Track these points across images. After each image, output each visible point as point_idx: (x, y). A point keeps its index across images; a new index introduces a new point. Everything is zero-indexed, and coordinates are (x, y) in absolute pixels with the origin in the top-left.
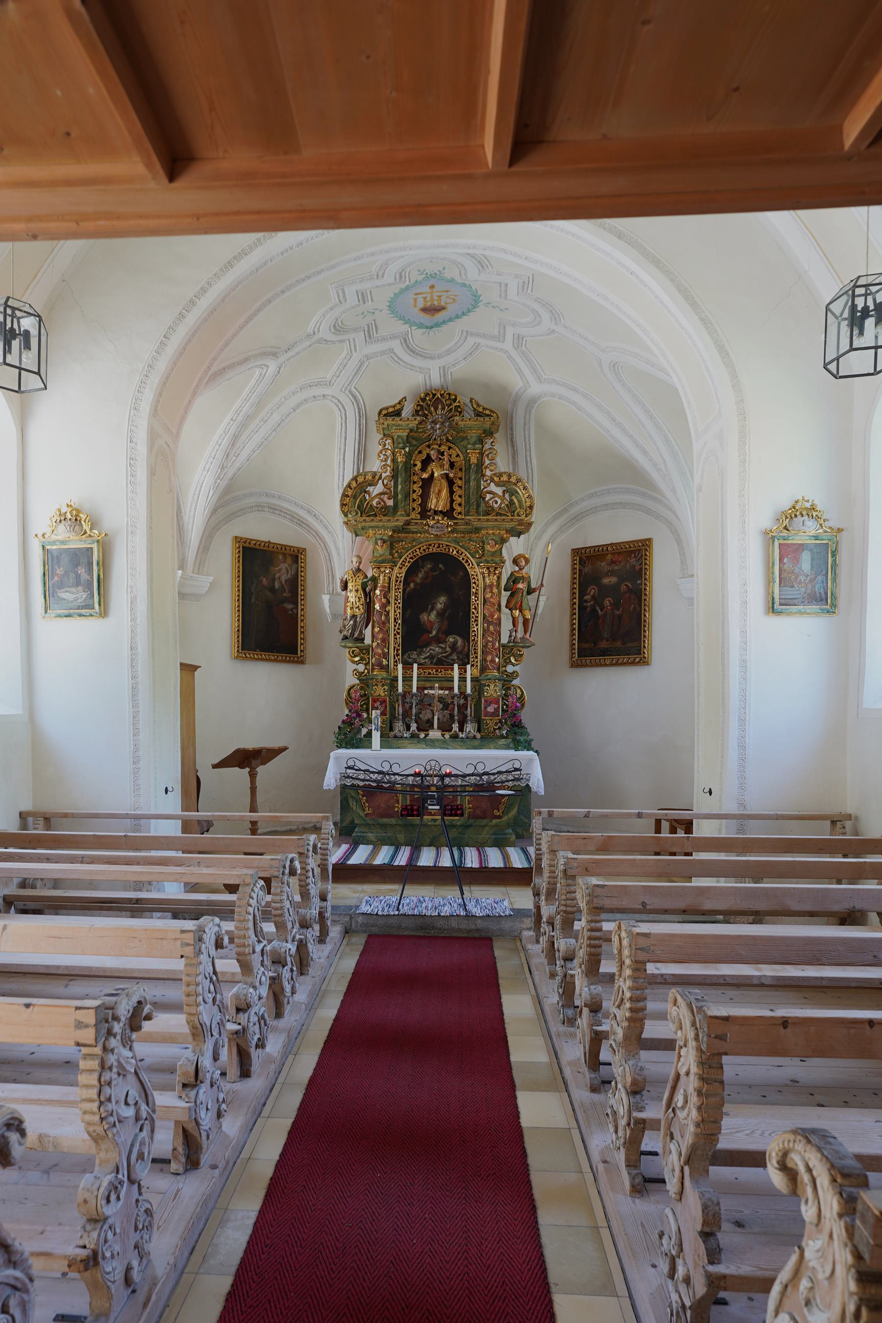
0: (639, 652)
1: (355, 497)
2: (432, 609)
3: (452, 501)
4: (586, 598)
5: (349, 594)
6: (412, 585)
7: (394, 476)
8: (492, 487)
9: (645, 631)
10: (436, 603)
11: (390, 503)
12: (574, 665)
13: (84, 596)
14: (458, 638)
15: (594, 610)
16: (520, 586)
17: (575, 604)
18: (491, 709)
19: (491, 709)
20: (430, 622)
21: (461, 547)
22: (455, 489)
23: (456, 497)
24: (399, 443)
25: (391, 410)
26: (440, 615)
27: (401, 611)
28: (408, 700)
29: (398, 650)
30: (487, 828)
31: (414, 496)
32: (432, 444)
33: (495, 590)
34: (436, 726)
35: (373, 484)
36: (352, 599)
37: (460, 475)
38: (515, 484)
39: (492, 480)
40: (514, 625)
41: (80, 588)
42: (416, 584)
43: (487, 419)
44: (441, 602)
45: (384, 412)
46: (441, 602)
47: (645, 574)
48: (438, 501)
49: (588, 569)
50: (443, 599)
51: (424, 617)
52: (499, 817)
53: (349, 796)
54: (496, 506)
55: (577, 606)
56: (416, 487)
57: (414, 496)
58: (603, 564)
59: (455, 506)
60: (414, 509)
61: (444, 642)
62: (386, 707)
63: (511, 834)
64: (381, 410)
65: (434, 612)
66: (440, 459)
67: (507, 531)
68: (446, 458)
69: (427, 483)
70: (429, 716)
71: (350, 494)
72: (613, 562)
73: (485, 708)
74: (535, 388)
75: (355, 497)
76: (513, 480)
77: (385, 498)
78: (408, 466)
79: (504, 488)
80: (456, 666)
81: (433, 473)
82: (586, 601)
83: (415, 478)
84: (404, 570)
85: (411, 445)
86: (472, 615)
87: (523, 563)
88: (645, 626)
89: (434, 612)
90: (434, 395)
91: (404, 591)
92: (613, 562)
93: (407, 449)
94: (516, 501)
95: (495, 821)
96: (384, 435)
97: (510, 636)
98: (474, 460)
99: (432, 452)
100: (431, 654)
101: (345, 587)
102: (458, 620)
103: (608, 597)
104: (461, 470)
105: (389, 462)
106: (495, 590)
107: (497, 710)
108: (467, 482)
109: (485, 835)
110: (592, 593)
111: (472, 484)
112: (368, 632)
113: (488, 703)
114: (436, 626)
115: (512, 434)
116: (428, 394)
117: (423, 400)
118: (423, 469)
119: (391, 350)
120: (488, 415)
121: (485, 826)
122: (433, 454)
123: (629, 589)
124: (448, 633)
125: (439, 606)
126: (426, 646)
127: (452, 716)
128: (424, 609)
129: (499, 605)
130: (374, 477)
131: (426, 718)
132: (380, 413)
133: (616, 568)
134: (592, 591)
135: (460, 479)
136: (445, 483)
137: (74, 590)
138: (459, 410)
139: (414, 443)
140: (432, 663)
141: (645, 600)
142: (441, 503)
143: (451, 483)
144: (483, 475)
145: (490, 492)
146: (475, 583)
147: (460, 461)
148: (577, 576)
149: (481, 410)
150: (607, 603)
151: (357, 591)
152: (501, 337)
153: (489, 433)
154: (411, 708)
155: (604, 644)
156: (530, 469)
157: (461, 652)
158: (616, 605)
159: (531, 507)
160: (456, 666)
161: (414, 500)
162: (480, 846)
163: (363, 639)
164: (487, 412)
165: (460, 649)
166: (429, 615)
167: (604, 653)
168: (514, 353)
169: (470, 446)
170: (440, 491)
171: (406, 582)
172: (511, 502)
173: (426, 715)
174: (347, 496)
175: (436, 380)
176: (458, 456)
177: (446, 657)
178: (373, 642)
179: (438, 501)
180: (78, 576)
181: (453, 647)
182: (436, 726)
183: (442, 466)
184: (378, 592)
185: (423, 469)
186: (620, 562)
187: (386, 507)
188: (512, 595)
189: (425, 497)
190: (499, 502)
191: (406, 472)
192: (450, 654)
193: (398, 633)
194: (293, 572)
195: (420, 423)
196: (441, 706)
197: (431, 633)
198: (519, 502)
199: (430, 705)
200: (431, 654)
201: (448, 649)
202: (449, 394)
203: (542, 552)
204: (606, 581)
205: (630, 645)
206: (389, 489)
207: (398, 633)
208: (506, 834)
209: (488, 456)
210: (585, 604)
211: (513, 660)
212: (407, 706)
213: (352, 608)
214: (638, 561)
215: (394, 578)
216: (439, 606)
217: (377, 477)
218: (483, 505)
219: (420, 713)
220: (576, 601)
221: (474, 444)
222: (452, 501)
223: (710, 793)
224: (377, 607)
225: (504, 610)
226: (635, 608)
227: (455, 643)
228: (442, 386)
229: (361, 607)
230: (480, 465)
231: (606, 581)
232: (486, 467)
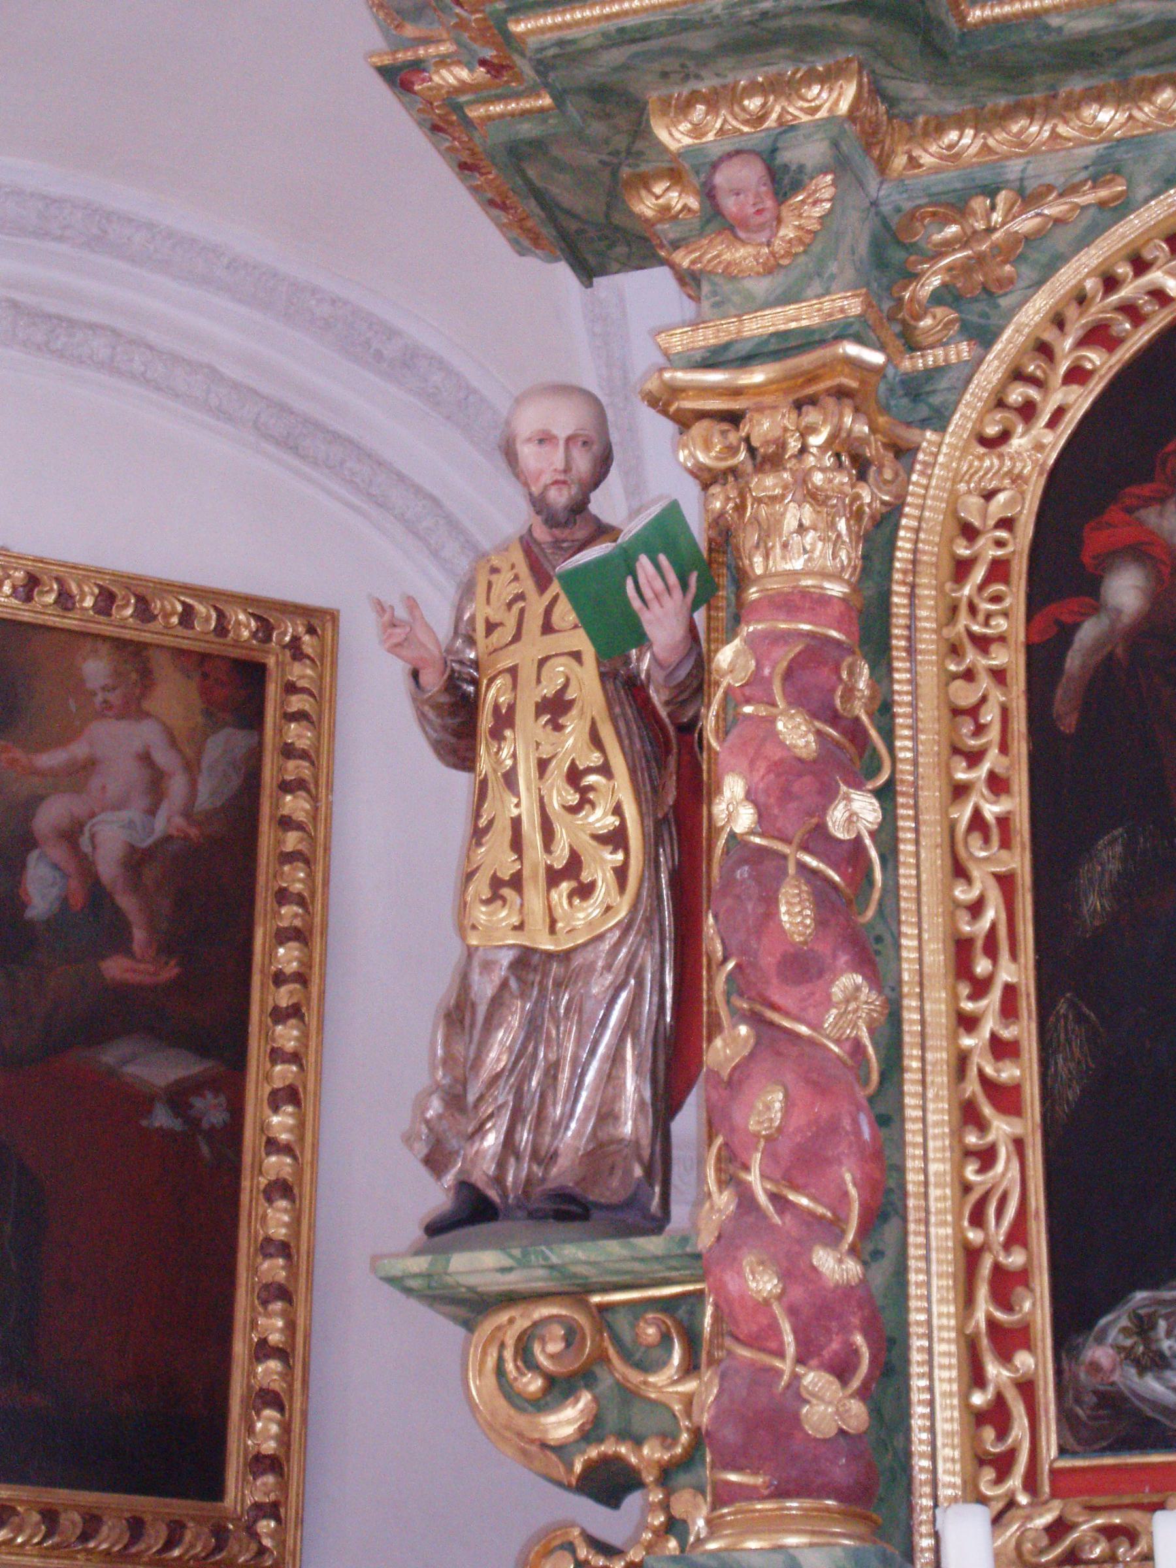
6: (1126, 590)
27: (1019, 862)
29: (1005, 1284)
84: (1036, 448)
91: (1044, 660)
171: (1060, 570)
193: (1006, 1098)
194: (209, 793)
207: (1006, 1098)
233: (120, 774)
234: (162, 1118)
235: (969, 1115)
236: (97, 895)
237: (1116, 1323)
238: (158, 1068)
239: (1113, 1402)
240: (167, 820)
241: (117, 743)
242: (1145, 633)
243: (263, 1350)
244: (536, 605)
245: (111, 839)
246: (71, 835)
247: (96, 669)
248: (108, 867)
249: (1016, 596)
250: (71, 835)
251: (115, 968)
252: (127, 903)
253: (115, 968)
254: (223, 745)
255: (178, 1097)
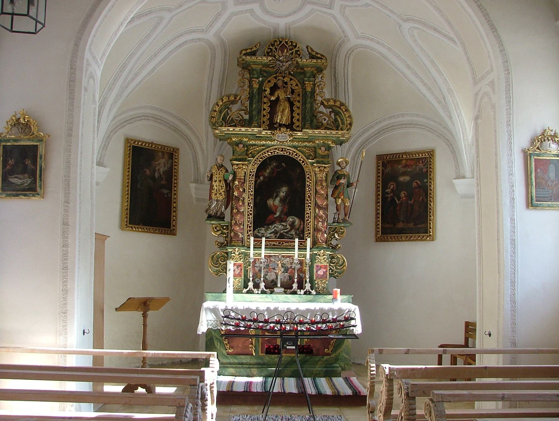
0: (426, 231)
1: (220, 112)
2: (276, 197)
3: (292, 117)
4: (387, 190)
5: (214, 183)
6: (262, 178)
7: (251, 98)
8: (322, 109)
9: (430, 216)
10: (279, 192)
11: (247, 117)
12: (378, 240)
13: (29, 182)
14: (296, 218)
15: (393, 200)
16: (342, 181)
17: (379, 195)
18: (321, 272)
19: (321, 272)
20: (275, 206)
21: (299, 151)
22: (295, 108)
23: (295, 115)
24: (255, 74)
25: (249, 51)
26: (282, 201)
28: (257, 265)
29: (250, 227)
30: (320, 363)
31: (264, 113)
32: (279, 76)
33: (324, 184)
34: (279, 285)
35: (233, 102)
36: (215, 187)
37: (298, 99)
38: (339, 108)
39: (322, 103)
40: (337, 210)
41: (26, 175)
42: (265, 177)
43: (319, 61)
44: (283, 191)
45: (243, 52)
46: (283, 191)
47: (430, 175)
48: (282, 117)
49: (388, 170)
50: (284, 189)
51: (270, 202)
52: (328, 354)
53: (214, 338)
54: (324, 122)
55: (380, 197)
56: (265, 106)
57: (264, 113)
58: (400, 167)
59: (295, 120)
60: (264, 122)
61: (286, 221)
62: (241, 270)
63: (338, 367)
64: (242, 51)
65: (278, 199)
66: (284, 87)
67: (333, 142)
68: (289, 86)
69: (274, 105)
70: (274, 277)
71: (217, 109)
72: (406, 166)
73: (317, 272)
74: (353, 41)
75: (220, 112)
76: (338, 104)
77: (242, 113)
78: (261, 90)
79: (331, 110)
80: (297, 240)
81: (278, 97)
82: (387, 193)
83: (265, 100)
84: (256, 166)
85: (263, 76)
86: (306, 202)
87: (345, 165)
88: (430, 212)
89: (278, 199)
90: (281, 42)
91: (256, 182)
92: (406, 166)
93: (261, 79)
94: (339, 120)
95: (325, 357)
96: (243, 68)
97: (334, 218)
98: (309, 89)
99: (278, 82)
100: (275, 230)
101: (211, 179)
102: (296, 206)
103: (403, 190)
104: (299, 95)
105: (246, 87)
106: (324, 184)
107: (325, 273)
108: (304, 104)
109: (318, 368)
110: (392, 187)
111: (308, 106)
112: (227, 213)
113: (319, 268)
114: (280, 209)
115: (335, 72)
116: (276, 41)
117: (273, 45)
118: (272, 94)
119: (252, 11)
120: (319, 58)
121: (318, 361)
122: (280, 83)
123: (419, 186)
124: (288, 214)
125: (282, 194)
126: (272, 224)
127: (291, 278)
128: (270, 196)
129: (327, 195)
130: (235, 98)
131: (271, 279)
132: (241, 53)
133: (409, 170)
134: (392, 185)
135: (299, 102)
136: (287, 105)
137: (21, 176)
138: (298, 54)
139: (265, 74)
140: (276, 237)
141: (430, 194)
142: (284, 119)
143: (292, 105)
144: (315, 100)
145: (321, 112)
146: (309, 178)
147: (298, 89)
148: (380, 175)
149: (314, 54)
150: (402, 194)
151: (220, 181)
152: (331, 7)
153: (320, 70)
154: (260, 271)
155: (400, 225)
156: (347, 97)
157: (298, 229)
158: (409, 197)
159: (351, 124)
160: (297, 240)
161: (264, 116)
162: (314, 376)
163: (224, 218)
164: (319, 56)
165: (297, 227)
166: (274, 201)
167: (401, 231)
168: (339, 17)
169: (306, 79)
170: (283, 111)
171: (257, 176)
172: (336, 120)
173: (271, 276)
174: (215, 111)
175: (282, 32)
176: (297, 85)
177: (287, 232)
178: (231, 220)
179: (282, 117)
180: (25, 166)
181: (292, 225)
182: (279, 285)
183: (285, 92)
184: (237, 183)
185: (272, 94)
186: (412, 166)
187: (243, 120)
188: (336, 188)
189: (273, 113)
190: (327, 119)
191: (259, 95)
192: (290, 231)
195: (270, 61)
196: (283, 270)
197: (275, 214)
198: (342, 120)
199: (274, 269)
200: (275, 230)
201: (288, 227)
202: (292, 42)
203: (357, 155)
204: (401, 179)
205: (419, 226)
206: (246, 107)
207: (251, 214)
208: (334, 367)
209: (318, 86)
210: (387, 195)
211: (336, 236)
212: (257, 269)
213: (216, 194)
214: (424, 165)
215: (248, 173)
216: (282, 194)
217: (238, 98)
218: (315, 121)
219: (267, 275)
220: (380, 193)
221: (309, 77)
222: (292, 117)
223: (490, 335)
224: (236, 194)
225: (330, 198)
226: (423, 199)
227: (293, 223)
228: (286, 36)
229: (223, 193)
230: (313, 92)
231: (401, 179)
232: (317, 94)
233: (162, 164)
234: (166, 196)
235: (248, 215)
236: (161, 175)
237: (257, 230)
238: (166, 191)
239: (256, 235)
240: (166, 169)
241: (162, 161)
242: (262, 181)
243: (174, 216)
244: (218, 172)
245: (162, 170)
246: (159, 170)
247: (160, 154)
248: (161, 173)
249: (254, 177)
250: (159, 170)
251: (162, 182)
252: (163, 176)
253: (162, 182)
254: (170, 161)
255: (167, 194)
